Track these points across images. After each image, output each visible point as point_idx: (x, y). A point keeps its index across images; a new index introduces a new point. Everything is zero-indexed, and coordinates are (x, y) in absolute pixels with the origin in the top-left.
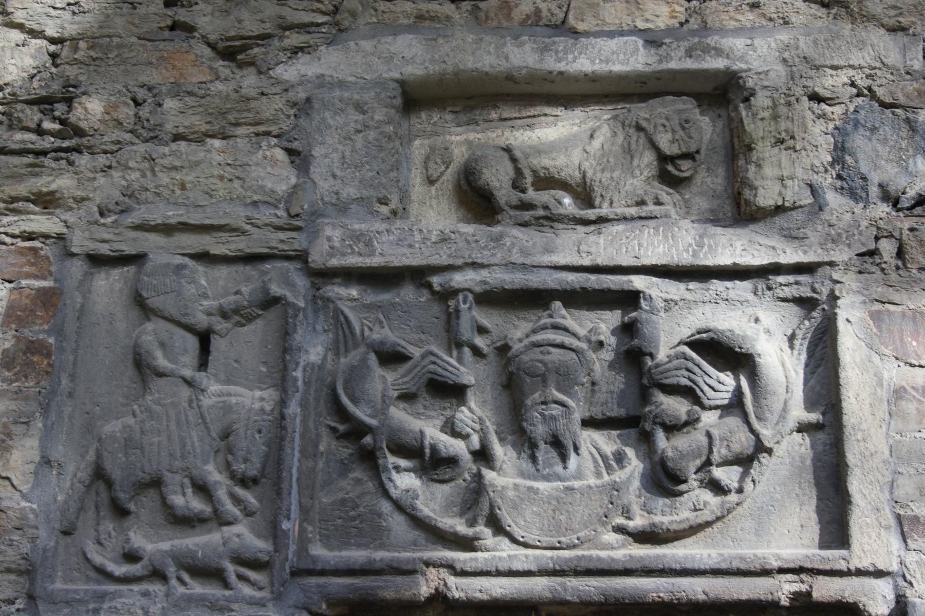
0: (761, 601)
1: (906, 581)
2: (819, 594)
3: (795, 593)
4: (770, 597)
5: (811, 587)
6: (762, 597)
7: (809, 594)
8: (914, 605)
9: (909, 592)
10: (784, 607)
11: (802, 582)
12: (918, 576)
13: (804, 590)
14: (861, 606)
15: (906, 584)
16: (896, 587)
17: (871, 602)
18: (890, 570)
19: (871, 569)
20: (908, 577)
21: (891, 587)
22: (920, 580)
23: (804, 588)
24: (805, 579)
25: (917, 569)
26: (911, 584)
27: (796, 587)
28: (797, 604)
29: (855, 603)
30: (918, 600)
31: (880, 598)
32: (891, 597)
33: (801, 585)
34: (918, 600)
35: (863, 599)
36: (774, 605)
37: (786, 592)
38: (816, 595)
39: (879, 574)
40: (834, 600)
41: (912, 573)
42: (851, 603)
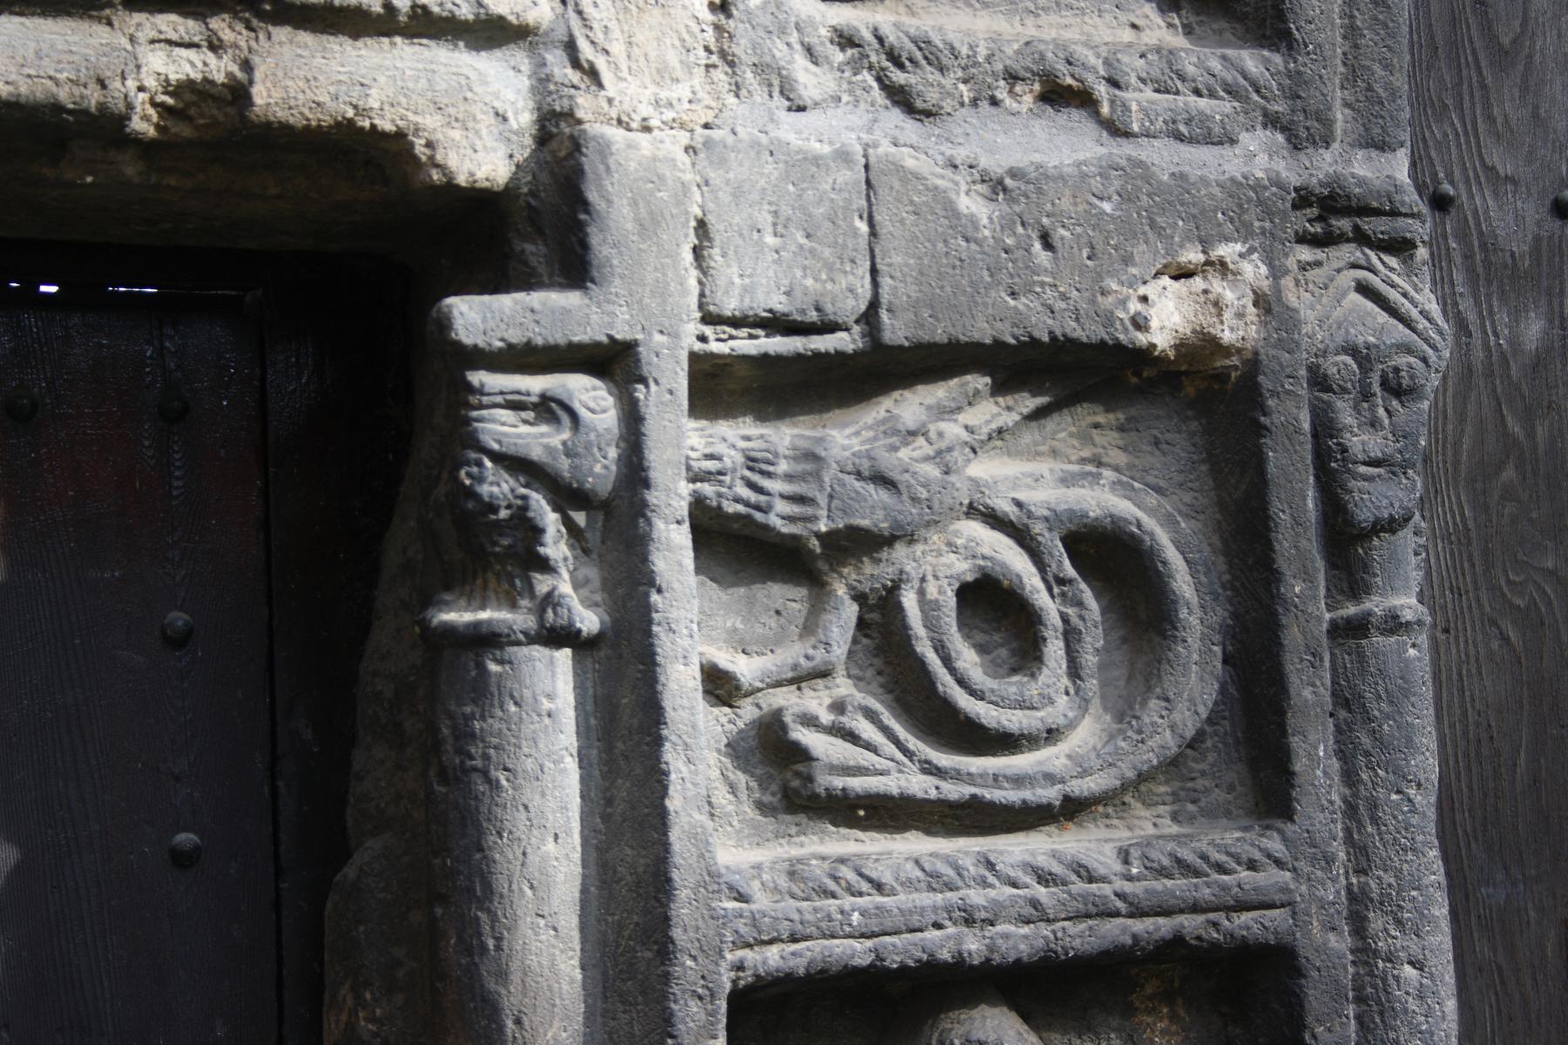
0: (57, 108)
1: (576, 63)
2: (277, 95)
3: (184, 89)
4: (93, 97)
5: (247, 66)
6: (64, 95)
7: (239, 93)
8: (604, 149)
9: (585, 105)
10: (137, 141)
11: (215, 46)
12: (617, 48)
13: (220, 78)
14: (420, 149)
15: (574, 76)
16: (542, 83)
17: (456, 134)
18: (531, 18)
19: (466, 12)
20: (586, 51)
21: (524, 82)
22: (624, 66)
23: (220, 68)
24: (227, 35)
25: (613, 25)
26: (593, 74)
27: (188, 65)
28: (184, 130)
29: (400, 135)
30: (616, 134)
31: (486, 120)
32: (523, 118)
33: (211, 58)
34: (616, 134)
35: (431, 122)
36: (105, 127)
37: (151, 83)
38: (265, 97)
39: (492, 33)
40: (327, 121)
41: (599, 36)
42: (384, 135)
